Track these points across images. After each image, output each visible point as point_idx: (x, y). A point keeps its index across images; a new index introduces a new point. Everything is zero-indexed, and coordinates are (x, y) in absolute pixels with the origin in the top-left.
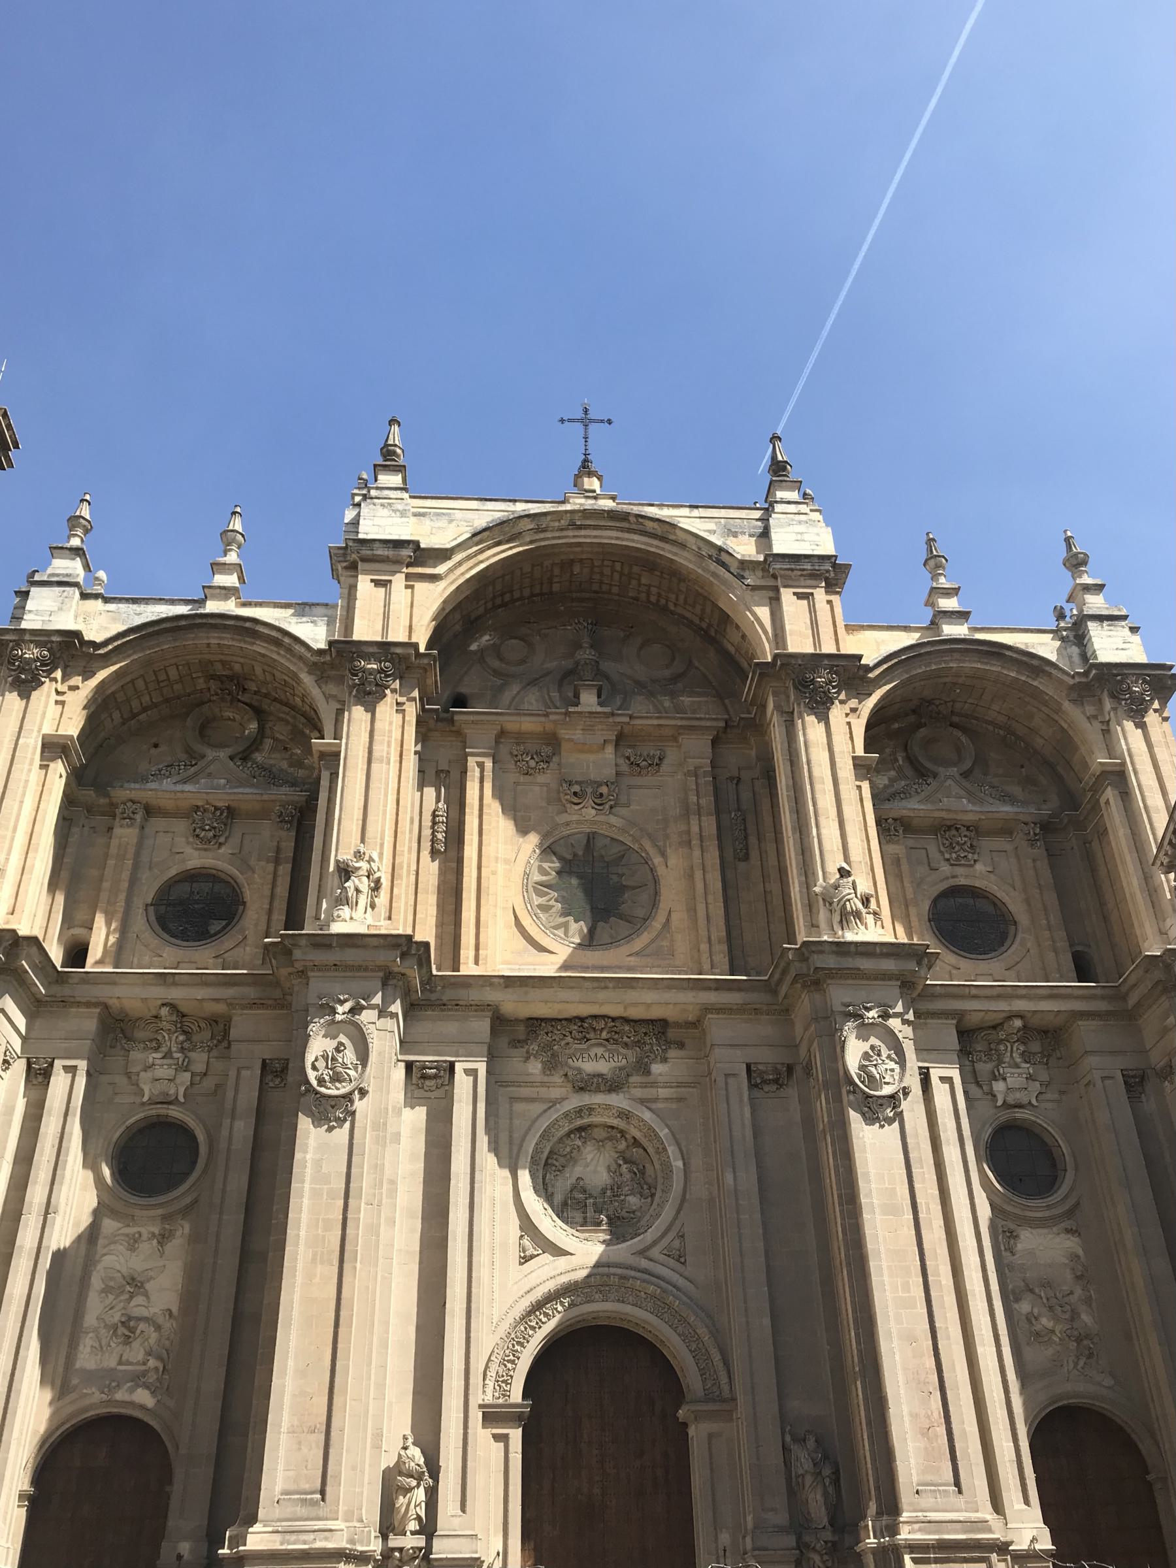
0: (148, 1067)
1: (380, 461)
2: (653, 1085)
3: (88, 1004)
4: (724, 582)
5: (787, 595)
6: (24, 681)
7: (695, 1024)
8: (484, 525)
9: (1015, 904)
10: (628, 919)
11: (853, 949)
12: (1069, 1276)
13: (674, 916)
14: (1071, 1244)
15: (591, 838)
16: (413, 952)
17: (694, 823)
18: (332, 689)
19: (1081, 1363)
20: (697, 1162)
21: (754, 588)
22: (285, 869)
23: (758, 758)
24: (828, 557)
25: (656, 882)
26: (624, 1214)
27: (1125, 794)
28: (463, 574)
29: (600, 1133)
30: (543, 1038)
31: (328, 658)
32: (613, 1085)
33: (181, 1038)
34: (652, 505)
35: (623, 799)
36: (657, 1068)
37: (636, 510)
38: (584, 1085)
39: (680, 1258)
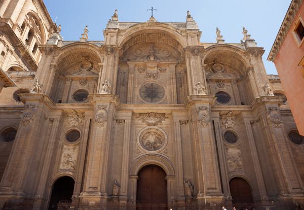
0: (71, 121)
2: (162, 124)
3: (59, 110)
4: (178, 35)
7: (171, 114)
9: (231, 95)
10: (159, 98)
12: (238, 156)
14: (239, 151)
15: (152, 84)
17: (172, 80)
18: (102, 55)
20: (170, 137)
24: (197, 30)
25: (164, 91)
29: (152, 133)
30: (142, 117)
32: (155, 125)
36: (163, 122)
38: (149, 125)
39: (166, 153)
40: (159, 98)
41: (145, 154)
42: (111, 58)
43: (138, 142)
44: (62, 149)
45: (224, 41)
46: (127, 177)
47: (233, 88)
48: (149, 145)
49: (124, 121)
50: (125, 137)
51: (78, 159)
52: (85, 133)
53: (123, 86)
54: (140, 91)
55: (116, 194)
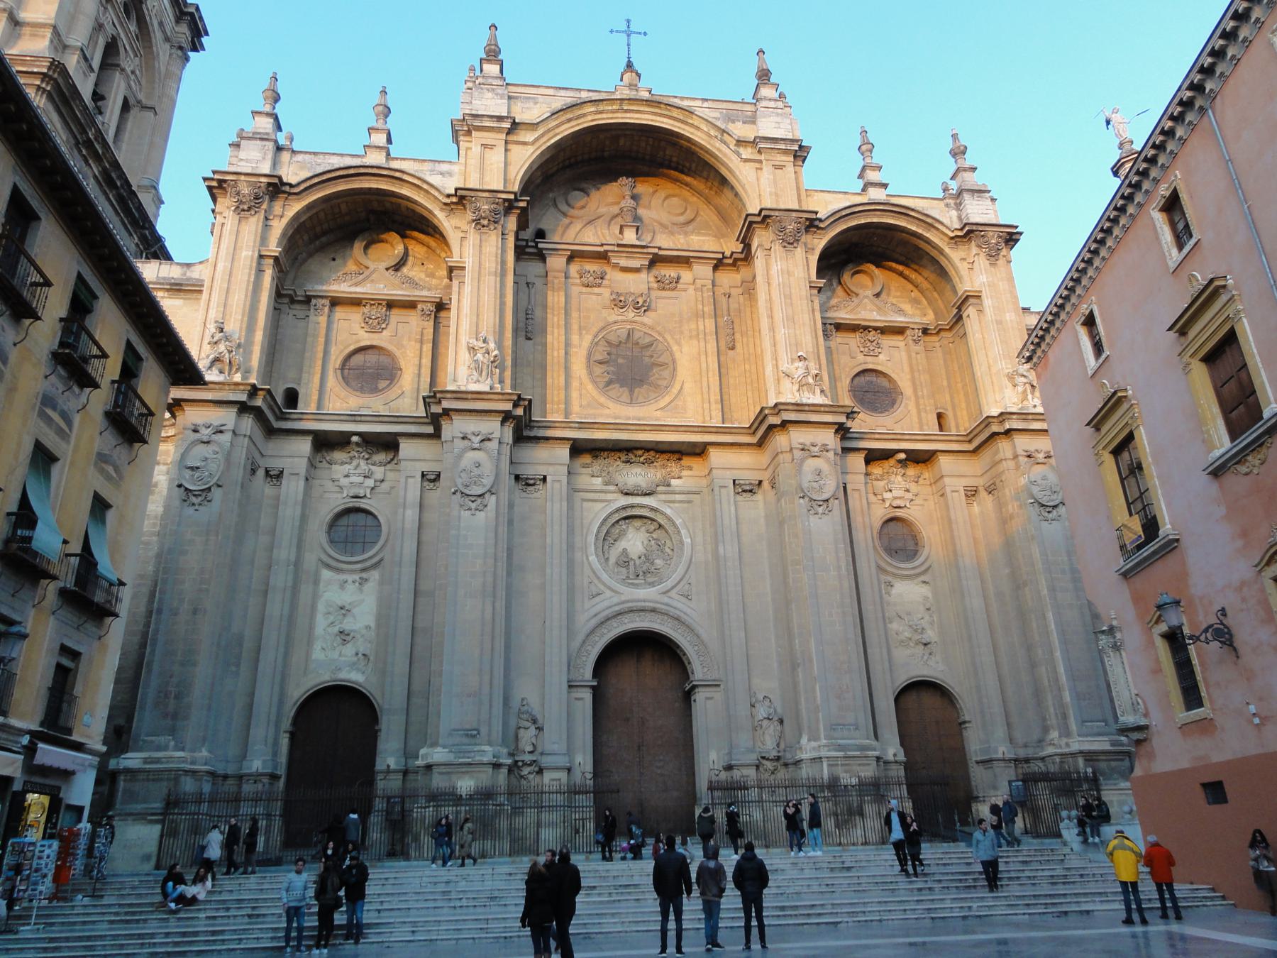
0: (347, 476)
1: (484, 56)
2: (674, 493)
4: (725, 155)
5: (767, 168)
6: (243, 210)
8: (560, 108)
9: (904, 383)
10: (657, 386)
11: (807, 408)
12: (922, 609)
13: (687, 386)
14: (925, 591)
16: (522, 403)
19: (925, 658)
21: (746, 161)
22: (428, 347)
23: (742, 282)
25: (674, 361)
26: (652, 570)
27: (980, 311)
28: (545, 143)
30: (601, 461)
31: (454, 199)
33: (367, 456)
34: (676, 97)
35: (653, 306)
36: (674, 482)
37: (665, 100)
40: (657, 386)
41: (615, 600)
42: (493, 239)
43: (593, 558)
44: (316, 582)
45: (885, 186)
46: (565, 686)
47: (910, 357)
48: (627, 567)
49: (544, 479)
50: (549, 540)
51: (378, 626)
52: (407, 526)
53: (530, 339)
54: (589, 359)
55: (530, 748)
